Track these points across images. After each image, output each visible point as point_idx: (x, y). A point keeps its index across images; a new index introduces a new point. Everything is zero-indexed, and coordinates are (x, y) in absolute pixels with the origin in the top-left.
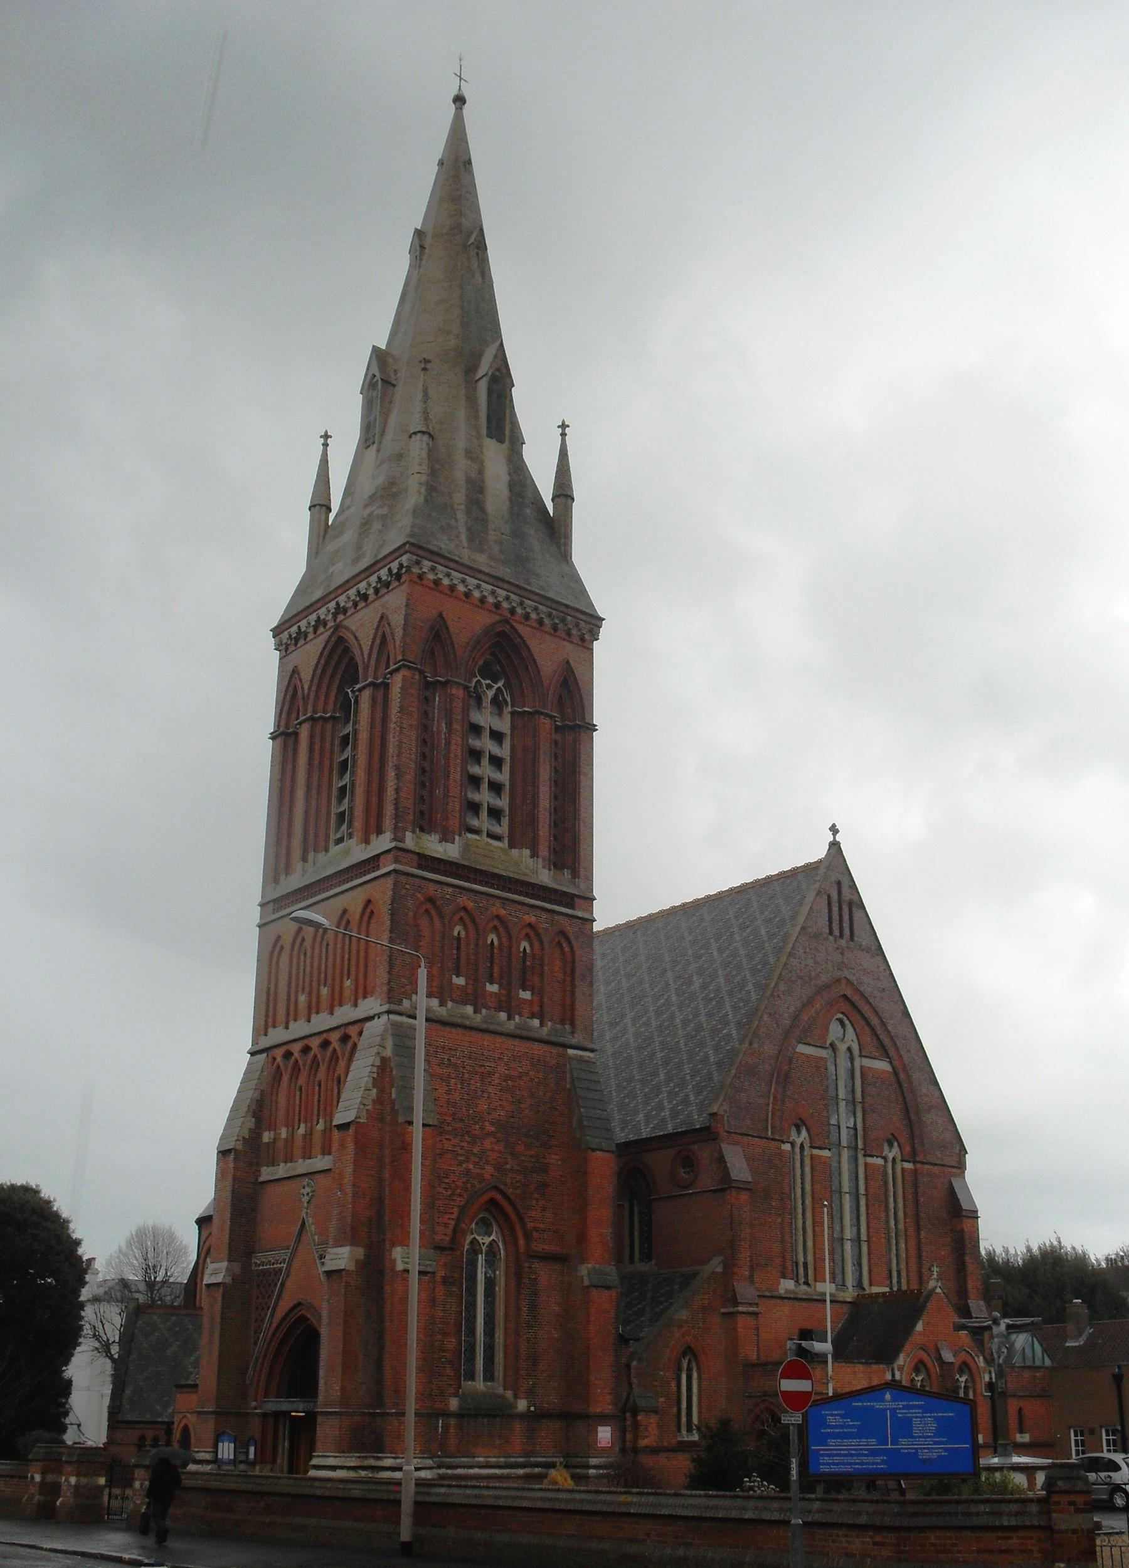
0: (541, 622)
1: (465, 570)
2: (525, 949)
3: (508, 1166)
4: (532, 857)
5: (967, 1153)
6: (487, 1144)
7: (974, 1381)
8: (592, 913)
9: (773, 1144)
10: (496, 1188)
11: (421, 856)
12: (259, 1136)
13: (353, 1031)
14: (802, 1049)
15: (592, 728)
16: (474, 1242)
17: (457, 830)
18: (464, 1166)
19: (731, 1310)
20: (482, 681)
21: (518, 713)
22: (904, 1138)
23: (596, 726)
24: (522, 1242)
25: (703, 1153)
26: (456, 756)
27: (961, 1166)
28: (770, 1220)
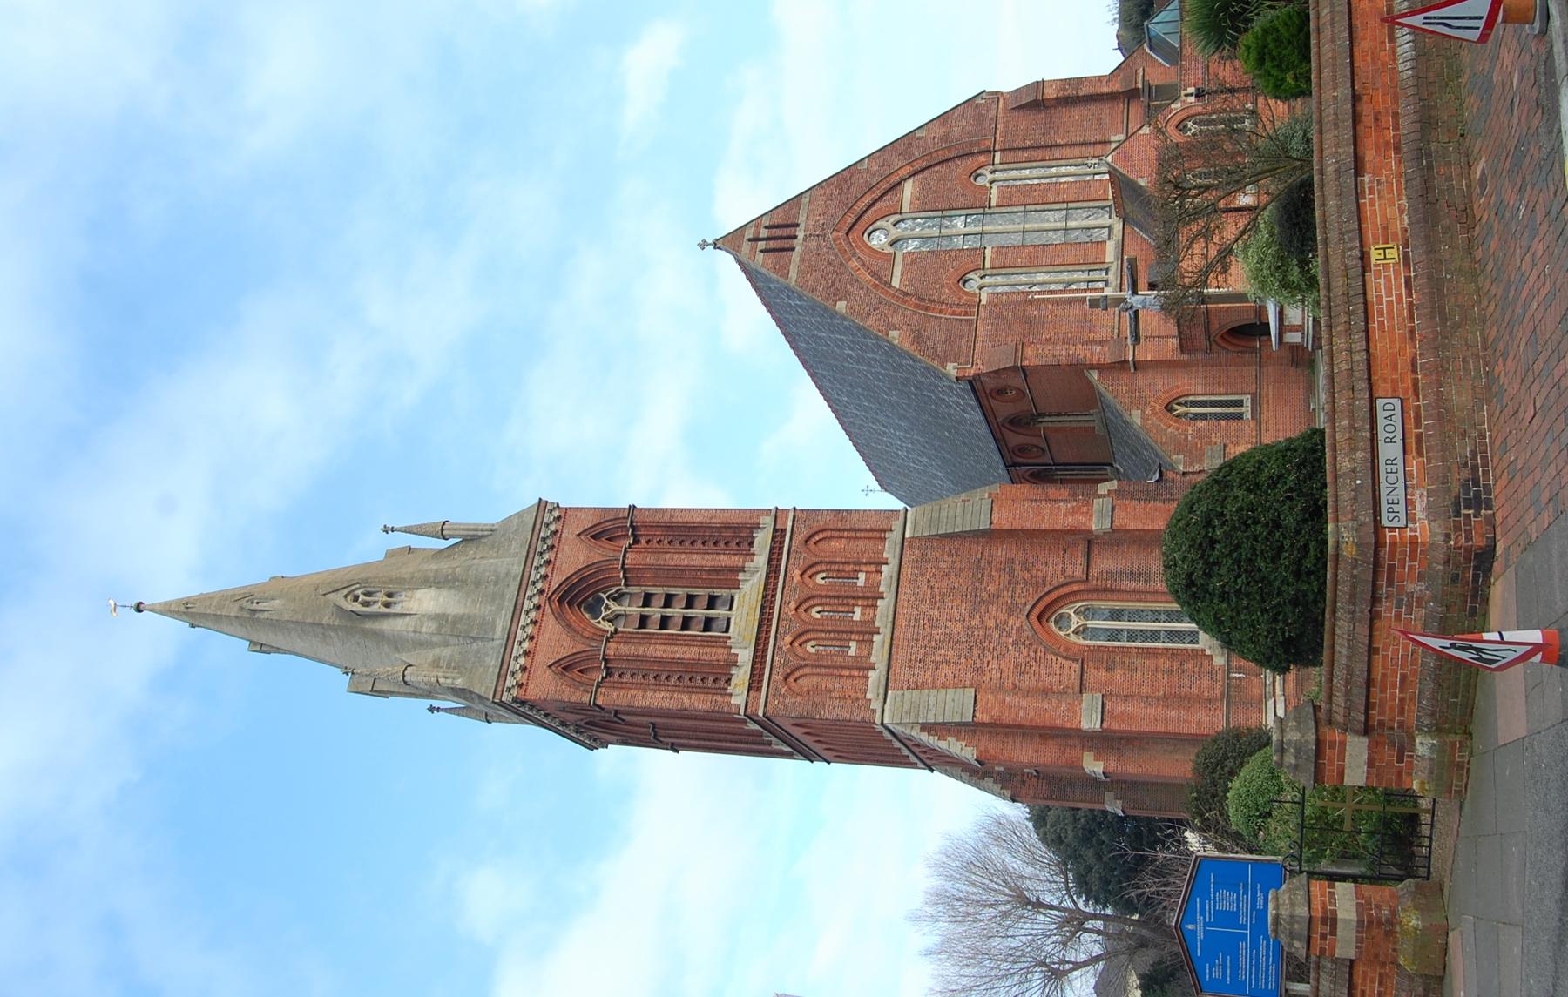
0: (548, 562)
1: (511, 641)
2: (823, 578)
3: (1009, 602)
4: (744, 571)
5: (984, 91)
6: (991, 623)
8: (787, 511)
9: (982, 314)
10: (1027, 616)
11: (750, 689)
12: (999, 773)
14: (896, 283)
15: (633, 508)
16: (1076, 632)
17: (726, 651)
18: (1010, 647)
19: (1131, 364)
20: (603, 614)
21: (625, 582)
22: (970, 163)
23: (630, 506)
24: (1075, 588)
25: (990, 384)
26: (665, 651)
27: (997, 95)
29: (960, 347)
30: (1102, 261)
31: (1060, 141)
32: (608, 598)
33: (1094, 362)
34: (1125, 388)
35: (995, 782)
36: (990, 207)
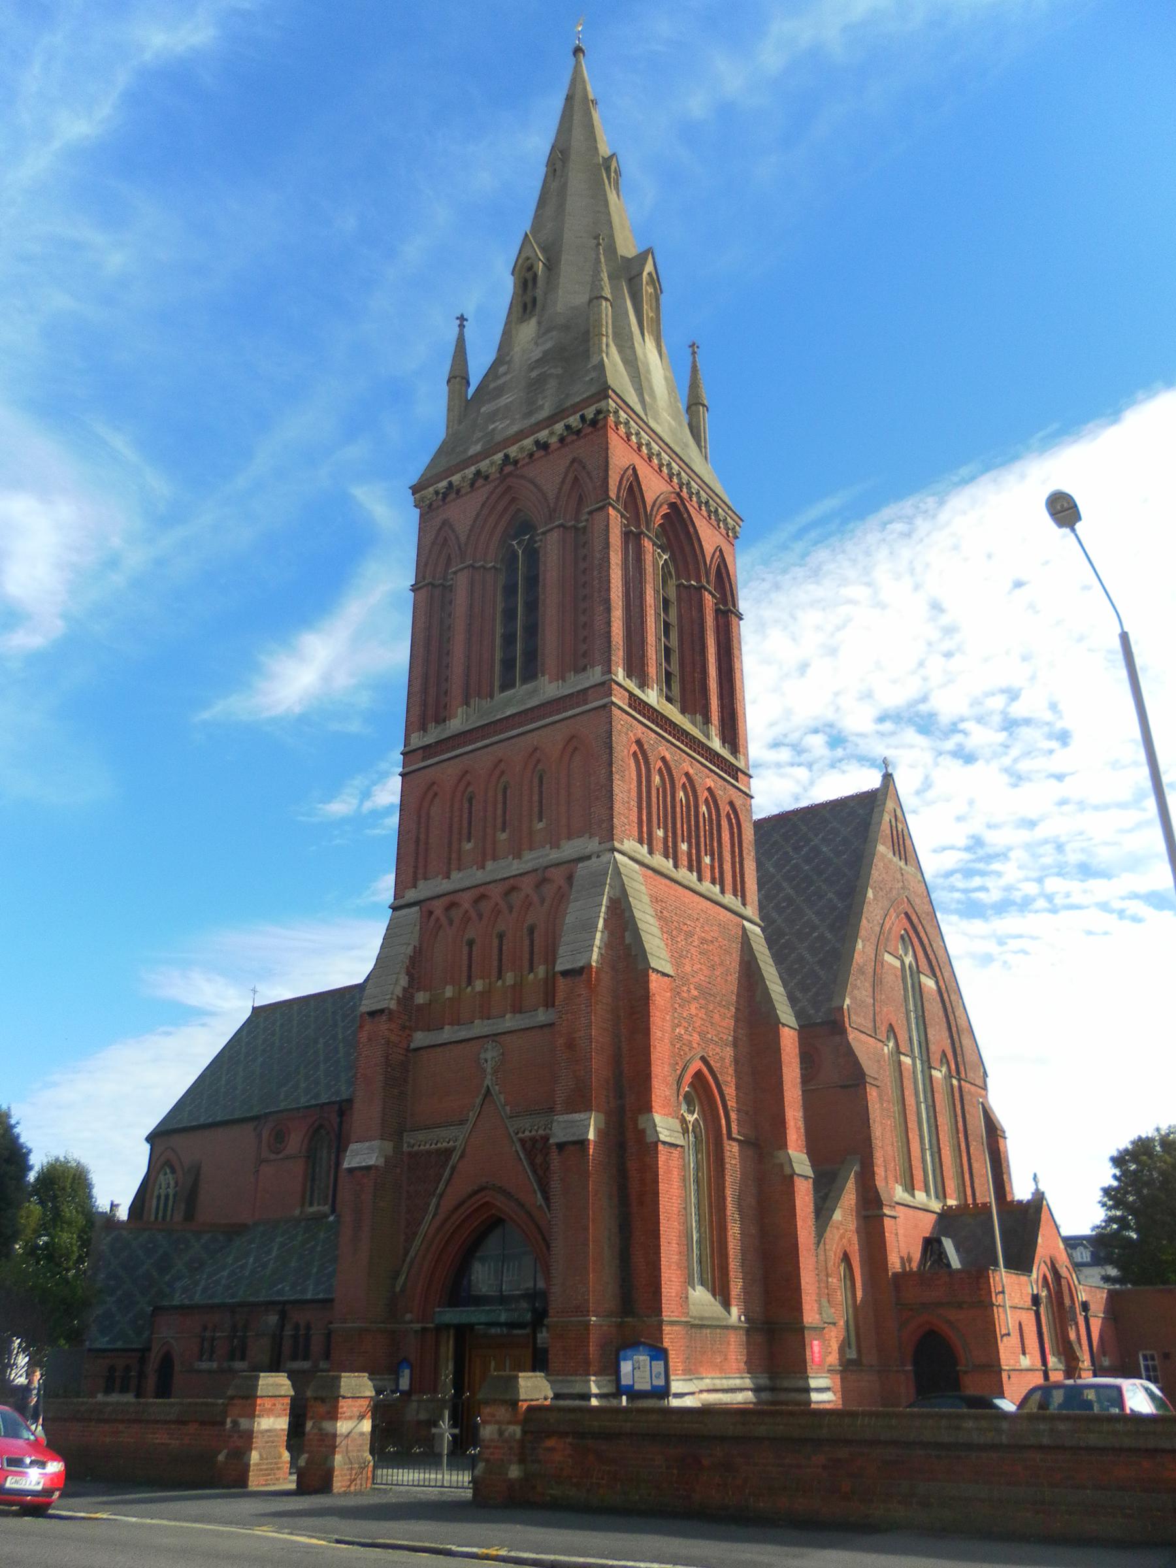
12: (412, 997)
13: (558, 875)
32: (666, 559)
35: (405, 989)
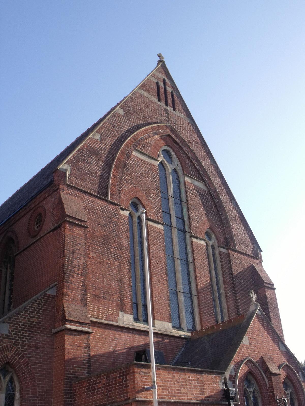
5: (261, 251)
7: (297, 393)
28: (108, 262)
29: (85, 181)
30: (155, 318)
31: (238, 297)
33: (65, 290)
34: (35, 320)
36: (192, 236)
